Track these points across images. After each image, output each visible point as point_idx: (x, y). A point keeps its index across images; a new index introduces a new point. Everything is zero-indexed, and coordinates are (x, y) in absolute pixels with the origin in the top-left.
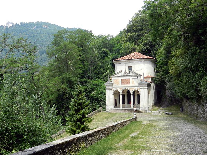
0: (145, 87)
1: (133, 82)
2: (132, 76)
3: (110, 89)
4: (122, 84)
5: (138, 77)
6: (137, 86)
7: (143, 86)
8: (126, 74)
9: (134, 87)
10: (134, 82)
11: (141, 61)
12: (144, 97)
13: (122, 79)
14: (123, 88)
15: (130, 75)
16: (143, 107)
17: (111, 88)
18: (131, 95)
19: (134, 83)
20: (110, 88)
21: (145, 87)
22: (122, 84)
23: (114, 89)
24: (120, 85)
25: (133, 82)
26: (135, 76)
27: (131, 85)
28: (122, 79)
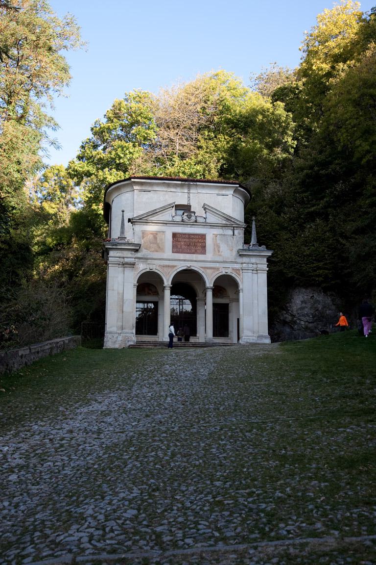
0: (259, 266)
1: (217, 247)
2: (213, 226)
3: (127, 264)
4: (173, 252)
5: (236, 232)
6: (232, 262)
7: (253, 260)
8: (193, 218)
9: (217, 265)
10: (219, 247)
11: (224, 192)
12: (256, 302)
13: (175, 235)
14: (181, 266)
15: (207, 221)
16: (251, 334)
17: (132, 260)
18: (205, 290)
19: (221, 249)
20: (126, 260)
21: (259, 266)
22: (173, 252)
23: (142, 267)
24: (168, 253)
25: (217, 247)
26: (224, 226)
27: (209, 255)
28: (175, 235)
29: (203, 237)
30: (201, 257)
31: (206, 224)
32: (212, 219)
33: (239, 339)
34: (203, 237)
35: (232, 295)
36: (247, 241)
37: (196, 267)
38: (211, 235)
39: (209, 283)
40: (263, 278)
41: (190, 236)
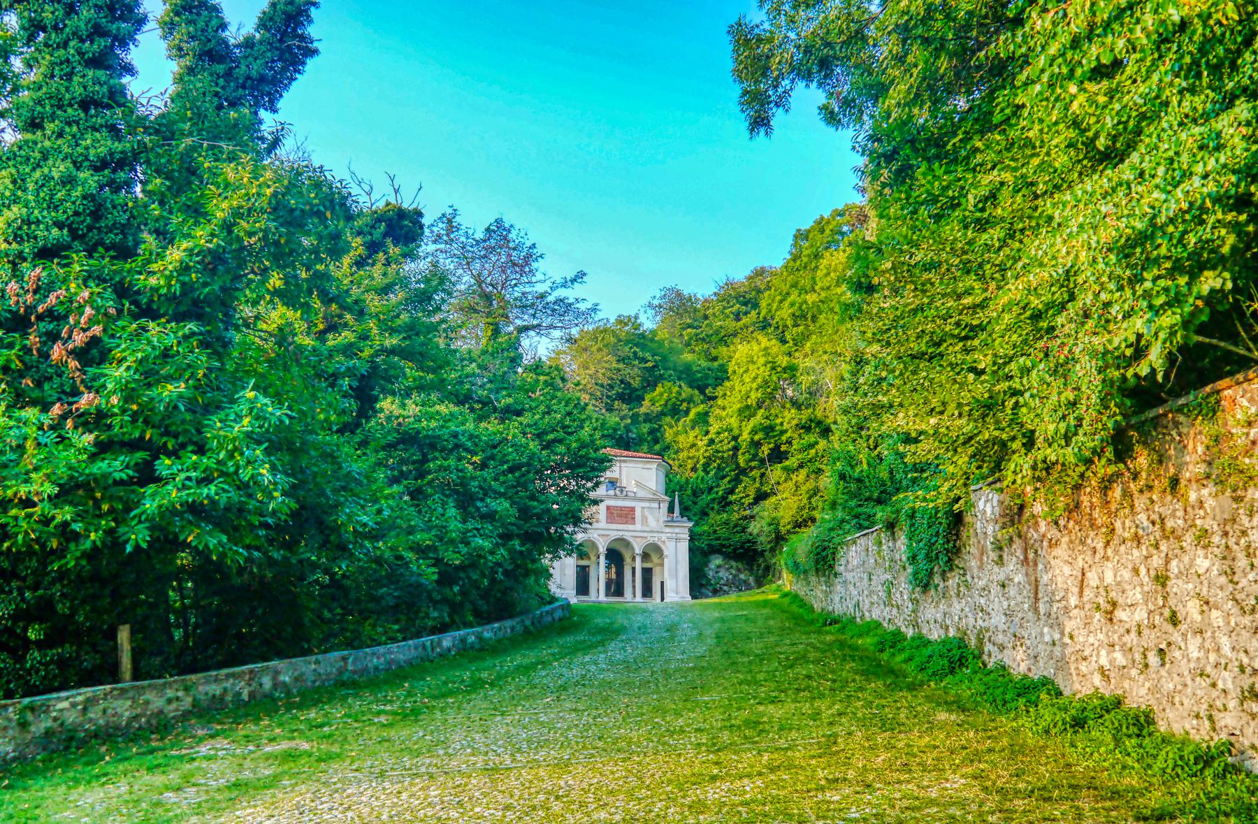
1: (644, 519)
7: (677, 530)
14: (615, 535)
28: (608, 508)
29: (633, 509)
30: (631, 527)
31: (636, 499)
32: (641, 494)
33: (662, 599)
34: (633, 509)
35: (655, 558)
36: (671, 510)
37: (627, 536)
38: (638, 506)
39: (638, 550)
40: (684, 547)
41: (621, 508)
